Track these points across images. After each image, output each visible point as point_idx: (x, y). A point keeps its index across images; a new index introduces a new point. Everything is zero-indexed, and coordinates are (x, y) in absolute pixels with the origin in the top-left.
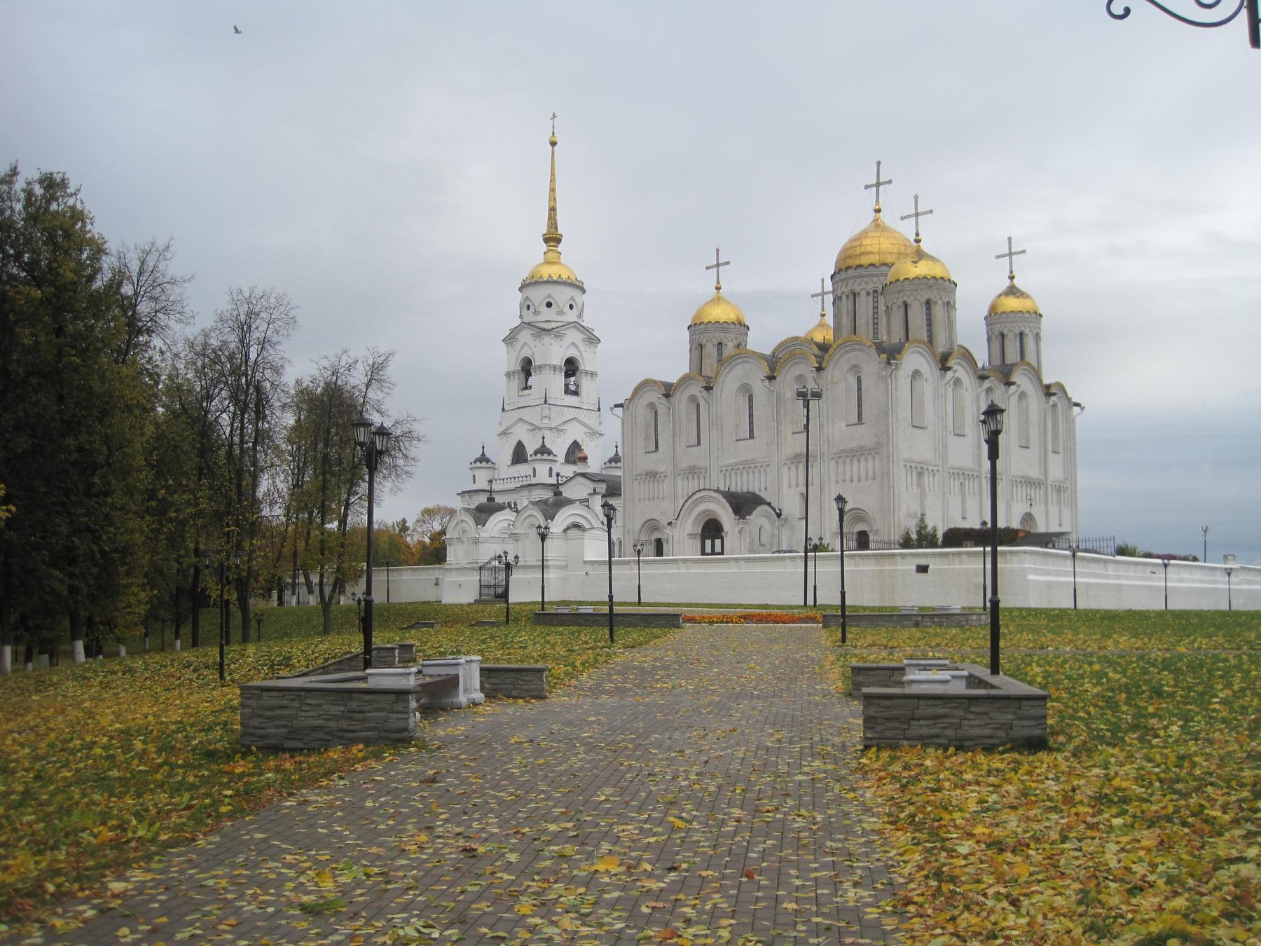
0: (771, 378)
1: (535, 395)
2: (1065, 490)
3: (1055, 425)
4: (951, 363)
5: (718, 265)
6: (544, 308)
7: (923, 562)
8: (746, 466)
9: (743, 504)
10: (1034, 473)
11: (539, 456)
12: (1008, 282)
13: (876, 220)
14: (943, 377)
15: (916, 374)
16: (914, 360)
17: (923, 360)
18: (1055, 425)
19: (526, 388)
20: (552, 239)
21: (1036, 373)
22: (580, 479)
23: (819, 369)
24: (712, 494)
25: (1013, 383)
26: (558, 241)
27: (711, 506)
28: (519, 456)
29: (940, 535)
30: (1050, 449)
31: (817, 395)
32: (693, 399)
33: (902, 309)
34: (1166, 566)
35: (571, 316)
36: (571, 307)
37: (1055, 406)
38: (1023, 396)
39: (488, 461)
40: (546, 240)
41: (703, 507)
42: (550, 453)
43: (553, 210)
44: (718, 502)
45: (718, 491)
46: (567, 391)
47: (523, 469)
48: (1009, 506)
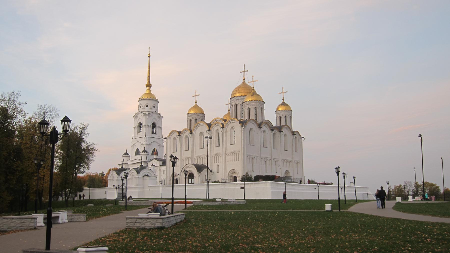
0: (209, 130)
2: (299, 164)
3: (296, 144)
4: (262, 126)
5: (196, 96)
9: (200, 168)
10: (290, 159)
11: (143, 153)
13: (244, 82)
15: (251, 129)
16: (250, 125)
17: (253, 125)
18: (296, 144)
19: (140, 132)
20: (149, 86)
21: (290, 128)
22: (154, 160)
23: (223, 128)
24: (191, 165)
26: (151, 87)
27: (191, 169)
28: (137, 153)
29: (253, 177)
31: (211, 138)
34: (318, 186)
35: (154, 110)
36: (154, 107)
38: (285, 135)
39: (128, 154)
40: (147, 86)
42: (146, 152)
43: (149, 77)
45: (193, 164)
46: (153, 133)
47: (139, 157)
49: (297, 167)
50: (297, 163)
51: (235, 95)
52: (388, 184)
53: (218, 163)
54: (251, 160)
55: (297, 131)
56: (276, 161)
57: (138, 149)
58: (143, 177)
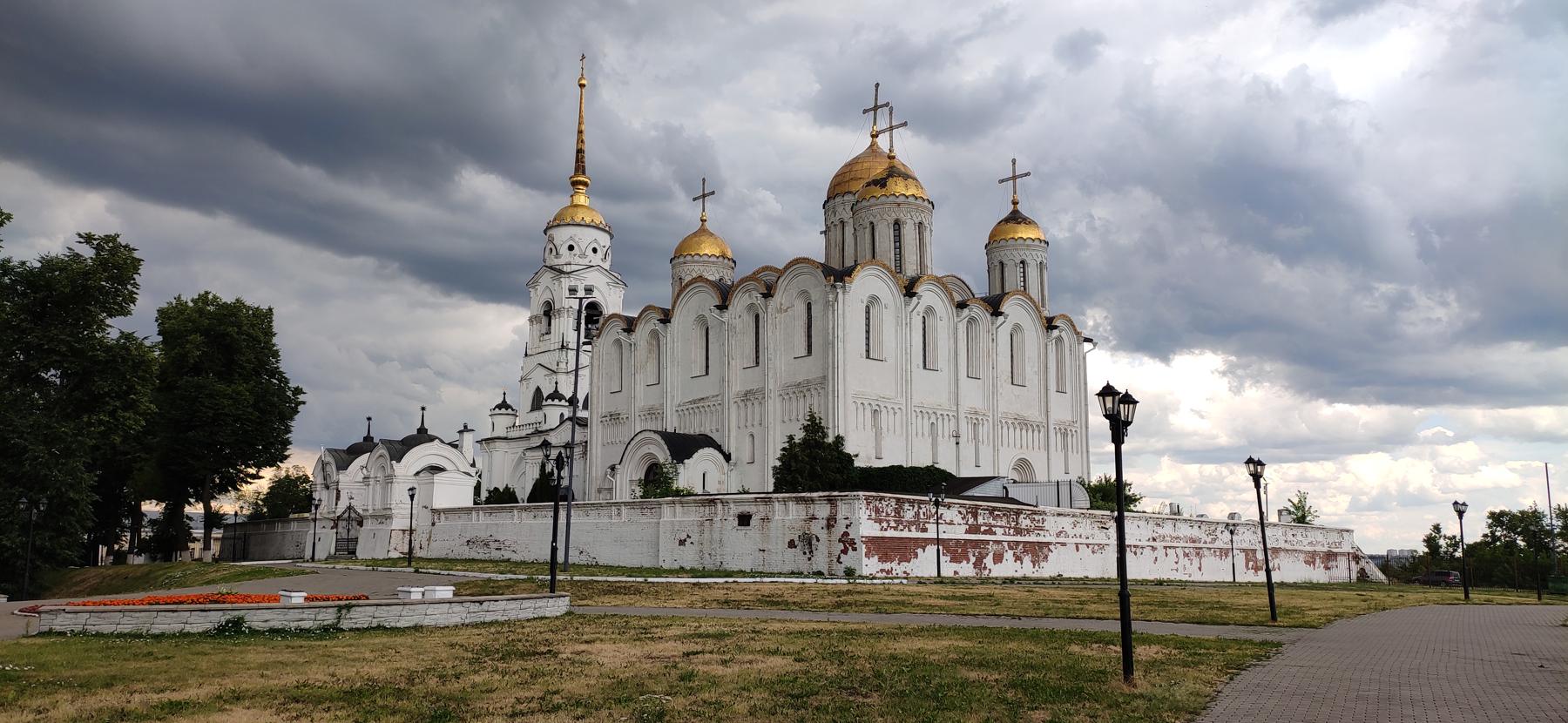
1: (554, 340)
4: (920, 289)
6: (564, 250)
7: (746, 509)
10: (1034, 414)
14: (907, 304)
25: (1001, 314)
27: (653, 449)
28: (538, 401)
30: (1053, 386)
32: (655, 335)
33: (868, 231)
35: (596, 259)
36: (595, 250)
37: (1059, 339)
41: (645, 450)
43: (580, 151)
44: (658, 445)
48: (995, 450)
49: (1065, 447)
50: (1065, 435)
52: (1461, 514)
53: (750, 430)
54: (869, 414)
55: (1064, 316)
56: (976, 421)
57: (538, 390)
58: (417, 473)
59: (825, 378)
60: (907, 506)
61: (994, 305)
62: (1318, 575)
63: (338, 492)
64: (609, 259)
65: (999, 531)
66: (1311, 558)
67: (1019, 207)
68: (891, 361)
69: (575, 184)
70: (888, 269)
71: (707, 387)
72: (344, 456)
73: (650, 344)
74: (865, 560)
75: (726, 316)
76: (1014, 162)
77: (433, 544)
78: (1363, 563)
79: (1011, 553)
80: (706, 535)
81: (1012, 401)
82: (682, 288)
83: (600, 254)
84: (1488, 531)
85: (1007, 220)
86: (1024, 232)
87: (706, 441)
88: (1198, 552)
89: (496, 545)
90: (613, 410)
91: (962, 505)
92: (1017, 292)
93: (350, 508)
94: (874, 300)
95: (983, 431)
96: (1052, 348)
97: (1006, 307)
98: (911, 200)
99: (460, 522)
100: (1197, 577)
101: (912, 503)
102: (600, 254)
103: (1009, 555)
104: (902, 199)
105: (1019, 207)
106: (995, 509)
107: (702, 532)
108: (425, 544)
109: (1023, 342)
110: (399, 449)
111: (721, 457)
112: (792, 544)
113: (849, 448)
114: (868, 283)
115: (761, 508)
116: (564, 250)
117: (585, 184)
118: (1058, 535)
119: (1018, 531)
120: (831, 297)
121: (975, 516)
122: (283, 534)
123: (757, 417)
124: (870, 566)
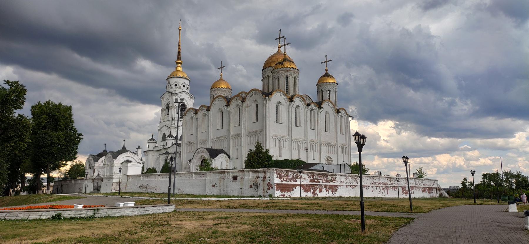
1: (170, 116)
4: (294, 99)
6: (173, 86)
8: (219, 139)
10: (332, 142)
12: (325, 72)
14: (290, 104)
25: (322, 108)
27: (204, 154)
28: (164, 138)
32: (204, 115)
33: (277, 80)
35: (184, 89)
36: (184, 86)
37: (341, 116)
40: (177, 63)
41: (201, 154)
43: (179, 52)
44: (206, 153)
47: (164, 143)
48: (320, 154)
49: (343, 152)
50: (343, 149)
51: (267, 66)
52: (473, 174)
53: (237, 147)
54: (277, 141)
55: (343, 109)
56: (313, 143)
57: (164, 134)
58: (122, 163)
59: (262, 130)
60: (290, 173)
61: (319, 105)
62: (426, 195)
63: (94, 170)
64: (189, 89)
65: (321, 181)
66: (424, 190)
67: (328, 72)
68: (285, 124)
69: (177, 63)
70: (284, 93)
71: (222, 133)
72: (97, 157)
73: (203, 118)
74: (276, 192)
75: (229, 108)
76: (326, 56)
77: (128, 188)
78: (441, 191)
79: (325, 189)
80: (222, 183)
81: (325, 137)
82: (214, 99)
83: (186, 87)
84: (482, 180)
85: (324, 76)
86: (330, 80)
87: (222, 151)
88: (387, 188)
89: (149, 188)
90: (190, 141)
91: (308, 173)
92: (327, 100)
93: (98, 175)
94: (279, 103)
95: (316, 147)
96: (339, 119)
97: (323, 105)
98: (292, 69)
99: (137, 180)
100: (386, 196)
101: (291, 172)
102: (186, 87)
103: (324, 189)
104: (289, 69)
105: (328, 72)
106: (319, 174)
107: (220, 183)
108: (124, 187)
109: (329, 117)
110: (116, 155)
111: (227, 157)
112: (251, 186)
113: (271, 153)
114: (277, 97)
115: (241, 174)
116: (173, 86)
117: (181, 63)
118: (341, 182)
119: (327, 181)
120: (264, 102)
121: (313, 176)
122: (75, 184)
123: (239, 143)
124: (278, 194)
